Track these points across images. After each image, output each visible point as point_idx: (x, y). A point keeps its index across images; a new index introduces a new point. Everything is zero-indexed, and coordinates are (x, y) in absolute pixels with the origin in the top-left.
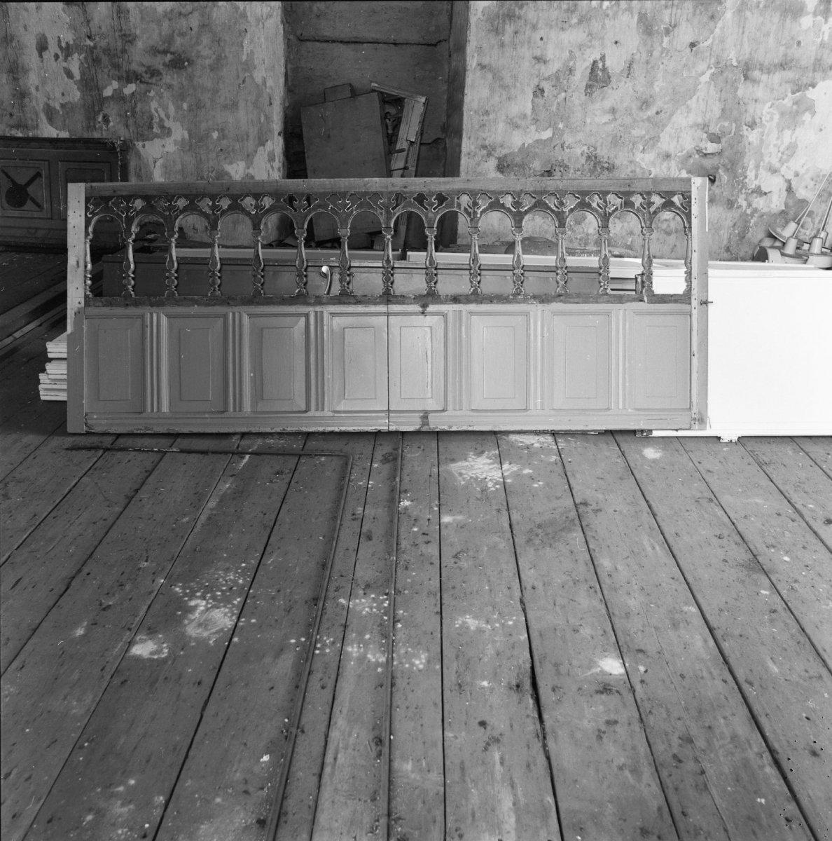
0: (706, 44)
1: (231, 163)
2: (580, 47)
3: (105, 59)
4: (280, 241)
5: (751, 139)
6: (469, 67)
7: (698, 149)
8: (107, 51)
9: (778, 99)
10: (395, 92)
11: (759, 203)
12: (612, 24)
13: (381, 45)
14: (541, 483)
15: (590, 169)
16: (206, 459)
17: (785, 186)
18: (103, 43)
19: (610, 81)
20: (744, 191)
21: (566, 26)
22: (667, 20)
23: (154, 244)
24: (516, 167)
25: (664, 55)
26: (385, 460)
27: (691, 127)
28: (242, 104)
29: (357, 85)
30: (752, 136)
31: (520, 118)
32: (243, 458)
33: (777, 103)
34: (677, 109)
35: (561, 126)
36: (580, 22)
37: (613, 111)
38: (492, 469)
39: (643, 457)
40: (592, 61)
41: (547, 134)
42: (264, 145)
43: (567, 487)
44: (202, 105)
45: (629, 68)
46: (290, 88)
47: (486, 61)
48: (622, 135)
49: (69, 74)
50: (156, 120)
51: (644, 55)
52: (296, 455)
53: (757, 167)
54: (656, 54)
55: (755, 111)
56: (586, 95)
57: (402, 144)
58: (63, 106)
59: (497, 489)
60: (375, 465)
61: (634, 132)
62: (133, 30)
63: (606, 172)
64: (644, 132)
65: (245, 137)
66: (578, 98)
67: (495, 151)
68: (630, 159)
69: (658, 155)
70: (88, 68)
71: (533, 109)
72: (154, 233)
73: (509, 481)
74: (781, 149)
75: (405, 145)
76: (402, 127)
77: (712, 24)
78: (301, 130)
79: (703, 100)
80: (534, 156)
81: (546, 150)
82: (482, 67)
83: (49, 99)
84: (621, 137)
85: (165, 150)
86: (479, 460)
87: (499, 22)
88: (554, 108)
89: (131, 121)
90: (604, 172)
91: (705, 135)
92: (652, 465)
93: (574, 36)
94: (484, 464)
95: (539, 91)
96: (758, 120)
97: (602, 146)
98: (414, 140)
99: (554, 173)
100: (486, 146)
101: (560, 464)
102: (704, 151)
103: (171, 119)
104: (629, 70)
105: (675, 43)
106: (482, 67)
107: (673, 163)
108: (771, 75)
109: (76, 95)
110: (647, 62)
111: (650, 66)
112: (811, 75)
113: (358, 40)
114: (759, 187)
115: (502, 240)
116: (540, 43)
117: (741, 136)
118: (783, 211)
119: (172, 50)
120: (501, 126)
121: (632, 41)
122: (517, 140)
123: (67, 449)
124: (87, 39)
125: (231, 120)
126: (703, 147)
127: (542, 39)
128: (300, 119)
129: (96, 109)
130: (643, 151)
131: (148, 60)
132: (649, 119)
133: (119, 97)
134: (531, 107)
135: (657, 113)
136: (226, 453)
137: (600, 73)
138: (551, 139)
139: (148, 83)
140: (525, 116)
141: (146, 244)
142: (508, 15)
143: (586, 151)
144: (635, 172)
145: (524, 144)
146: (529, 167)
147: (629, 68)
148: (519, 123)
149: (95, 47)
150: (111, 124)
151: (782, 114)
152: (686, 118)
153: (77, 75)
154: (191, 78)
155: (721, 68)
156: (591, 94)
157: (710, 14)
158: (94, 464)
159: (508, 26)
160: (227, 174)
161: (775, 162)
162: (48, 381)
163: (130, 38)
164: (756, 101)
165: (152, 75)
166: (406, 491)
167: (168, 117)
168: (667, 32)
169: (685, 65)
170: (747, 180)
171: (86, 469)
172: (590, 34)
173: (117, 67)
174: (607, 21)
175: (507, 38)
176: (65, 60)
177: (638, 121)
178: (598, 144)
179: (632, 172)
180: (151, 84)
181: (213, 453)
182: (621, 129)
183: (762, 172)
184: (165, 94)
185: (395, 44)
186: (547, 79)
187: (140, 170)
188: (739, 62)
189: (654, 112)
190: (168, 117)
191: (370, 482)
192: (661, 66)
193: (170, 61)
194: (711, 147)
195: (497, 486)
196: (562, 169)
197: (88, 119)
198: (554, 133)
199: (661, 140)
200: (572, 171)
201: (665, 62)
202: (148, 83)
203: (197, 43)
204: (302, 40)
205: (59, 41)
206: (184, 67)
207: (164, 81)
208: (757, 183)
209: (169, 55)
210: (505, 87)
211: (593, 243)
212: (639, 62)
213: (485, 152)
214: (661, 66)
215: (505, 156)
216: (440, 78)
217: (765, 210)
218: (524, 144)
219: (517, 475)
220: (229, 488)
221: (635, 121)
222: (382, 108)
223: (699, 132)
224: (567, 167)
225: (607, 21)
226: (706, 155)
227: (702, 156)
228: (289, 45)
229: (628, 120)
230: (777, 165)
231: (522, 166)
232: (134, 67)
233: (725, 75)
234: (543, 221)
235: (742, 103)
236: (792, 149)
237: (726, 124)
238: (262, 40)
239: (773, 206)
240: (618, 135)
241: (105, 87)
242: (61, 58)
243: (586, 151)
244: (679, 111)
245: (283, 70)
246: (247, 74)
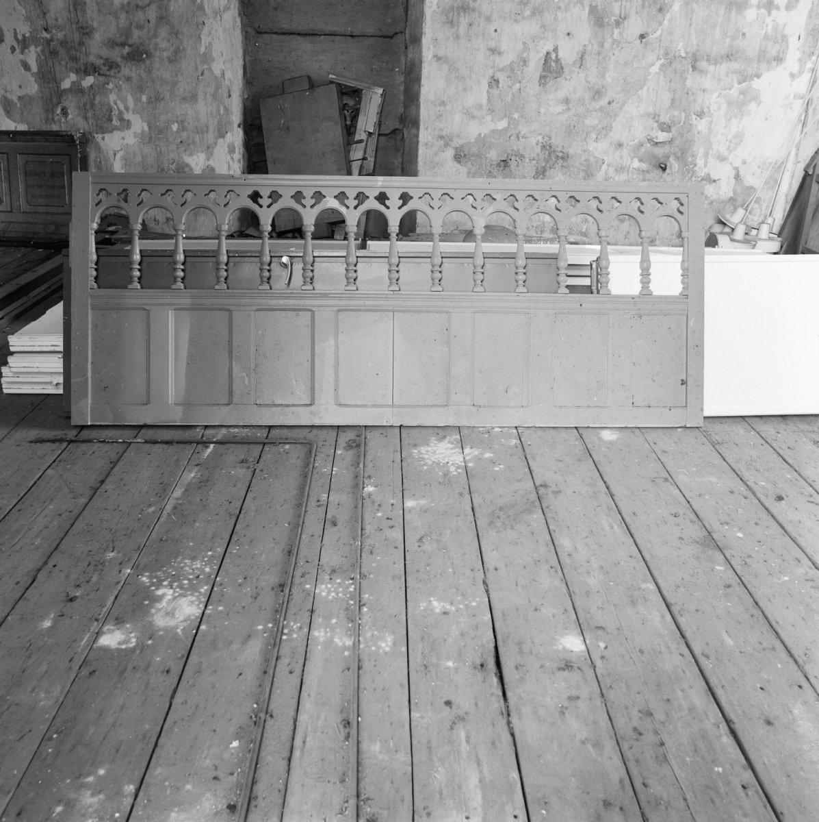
0: (655, 35)
1: (191, 155)
2: (534, 39)
3: (62, 52)
4: (242, 232)
5: (700, 128)
6: (424, 59)
7: (649, 138)
8: (64, 43)
9: (725, 90)
10: (353, 84)
11: (710, 190)
12: (563, 16)
13: (338, 37)
14: (502, 466)
15: (545, 158)
16: (171, 450)
17: (733, 173)
18: (60, 35)
19: (563, 72)
20: (693, 179)
21: (519, 18)
22: (617, 12)
23: (115, 236)
25: (615, 46)
26: (349, 446)
27: (643, 116)
28: (201, 97)
29: (313, 76)
30: (701, 125)
32: (207, 447)
33: (724, 92)
34: (628, 99)
35: (516, 116)
36: (533, 14)
37: (567, 101)
38: (452, 453)
39: (600, 439)
40: (545, 53)
41: (502, 125)
42: (224, 137)
43: (527, 470)
44: (161, 97)
45: (582, 58)
46: (248, 81)
47: (441, 53)
49: (26, 67)
50: (116, 112)
51: (596, 47)
52: (260, 443)
53: (706, 155)
54: (607, 45)
55: (703, 100)
56: (540, 85)
57: (360, 135)
58: (20, 98)
59: (459, 473)
60: (339, 452)
61: (587, 122)
62: (90, 22)
63: (561, 161)
64: (596, 122)
65: (205, 129)
66: (532, 88)
67: (452, 141)
69: (611, 144)
70: (46, 59)
71: (489, 100)
72: (115, 225)
73: (470, 465)
74: (729, 138)
75: (364, 136)
76: (361, 118)
77: (660, 16)
78: (261, 123)
79: (653, 90)
81: (501, 140)
82: (438, 58)
83: (6, 91)
84: (575, 126)
85: (126, 142)
86: (441, 444)
87: (453, 15)
88: (509, 99)
89: (89, 114)
91: (656, 124)
92: (609, 446)
93: (528, 28)
94: (446, 448)
95: (494, 82)
96: (706, 110)
98: (372, 131)
99: (510, 163)
100: (443, 137)
101: (520, 447)
102: (655, 141)
103: (131, 112)
104: (582, 62)
105: (625, 35)
106: (438, 58)
107: (625, 152)
108: (718, 66)
109: (33, 88)
110: (599, 54)
111: (601, 58)
112: (755, 65)
113: (315, 32)
114: (709, 174)
115: (460, 228)
116: (494, 34)
117: (691, 125)
118: (732, 197)
119: (130, 42)
120: (458, 117)
121: (585, 33)
122: (474, 130)
123: (31, 442)
124: (43, 31)
125: (190, 112)
126: (654, 136)
127: (496, 30)
128: (259, 111)
129: (55, 101)
130: (596, 140)
131: (105, 52)
132: (601, 109)
133: (77, 90)
135: (609, 103)
136: (190, 442)
137: (553, 64)
138: (506, 130)
139: (106, 76)
140: (480, 107)
141: (107, 236)
142: (463, 7)
143: (541, 140)
144: (589, 161)
147: (582, 58)
148: (475, 113)
149: (51, 40)
150: (70, 117)
151: (730, 104)
152: (637, 107)
153: (34, 68)
154: (149, 71)
155: (670, 59)
156: (544, 85)
157: (658, 6)
158: (59, 456)
159: (463, 18)
160: (188, 165)
161: (723, 151)
162: (11, 375)
163: (87, 31)
164: (704, 91)
165: (110, 68)
166: (369, 477)
167: (127, 109)
168: (618, 24)
169: (636, 57)
170: (696, 168)
171: (51, 462)
172: (543, 26)
173: (75, 59)
174: (559, 14)
175: (462, 29)
176: (22, 53)
177: (591, 111)
179: (586, 161)
180: (109, 76)
181: (177, 443)
182: (575, 118)
183: (711, 160)
184: (123, 87)
185: (352, 36)
186: (502, 70)
187: (100, 162)
188: (687, 53)
189: (606, 102)
190: (127, 109)
191: (334, 469)
192: (613, 58)
193: (128, 54)
194: (662, 136)
195: (460, 471)
196: (517, 159)
197: (47, 111)
198: (509, 123)
199: (614, 129)
201: (616, 52)
202: (106, 76)
203: (155, 36)
204: (259, 32)
205: (16, 34)
206: (143, 60)
207: (122, 73)
208: (706, 170)
209: (127, 47)
210: (461, 78)
211: (549, 231)
212: (591, 52)
213: (442, 142)
214: (613, 58)
215: (462, 146)
216: (397, 70)
217: (715, 197)
219: (478, 459)
220: (194, 478)
221: (588, 111)
222: (340, 99)
223: (651, 122)
224: (522, 156)
225: (559, 14)
226: (657, 143)
227: (653, 145)
228: (247, 38)
229: (581, 110)
230: (726, 153)
231: (479, 156)
232: (92, 59)
233: (674, 65)
235: (689, 92)
236: (739, 137)
237: (676, 113)
238: (221, 33)
239: (722, 193)
241: (64, 79)
242: (18, 50)
243: (541, 140)
244: (630, 101)
245: (241, 62)
246: (205, 67)
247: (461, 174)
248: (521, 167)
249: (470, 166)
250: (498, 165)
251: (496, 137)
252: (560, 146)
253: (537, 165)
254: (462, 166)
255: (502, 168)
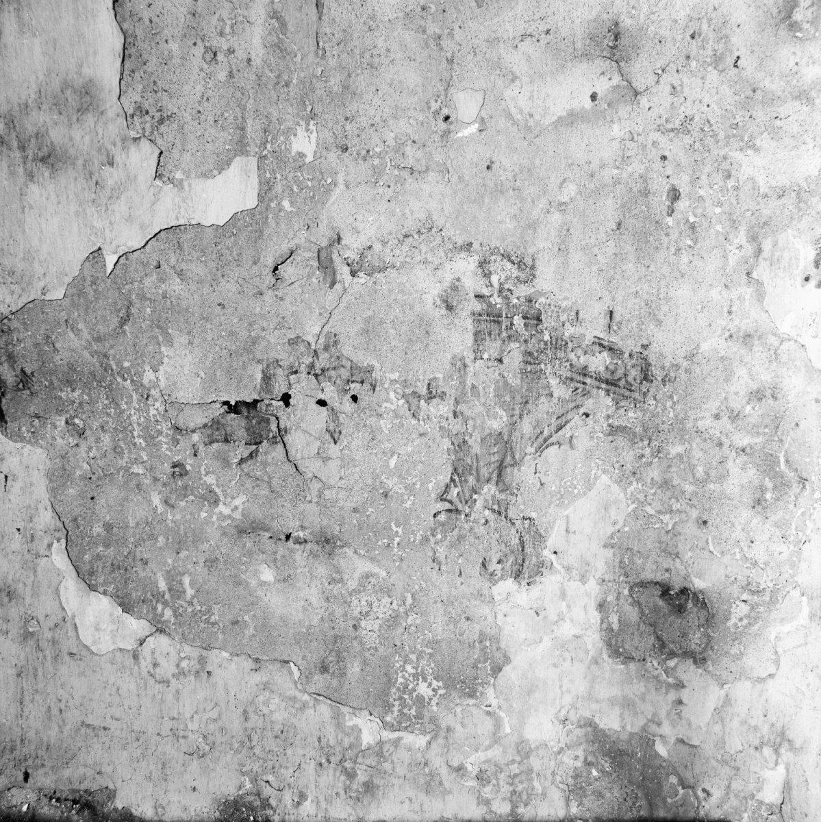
24: (69, 383)
31: (58, 105)
35: (304, 143)
48: (683, 183)
61: (751, 166)
63: (601, 403)
68: (742, 324)
80: (160, 325)
81: (229, 288)
84: (675, 195)
88: (254, 41)
90: (589, 404)
97: (562, 250)
134: (115, 41)
143: (472, 283)
145: (96, 254)
146: (138, 385)
148: (56, 135)
177: (772, 100)
178: (542, 245)
179: (757, 395)
196: (329, 393)
198: (266, 190)
200: (393, 401)
218: (96, 254)
234: (257, 678)
240: (660, 187)
243: (472, 283)
247: (16, 487)
248: (355, 441)
249: (64, 441)
250: (216, 432)
251: (197, 269)
252: (594, 316)
253: (456, 426)
254: (17, 437)
255: (243, 451)
